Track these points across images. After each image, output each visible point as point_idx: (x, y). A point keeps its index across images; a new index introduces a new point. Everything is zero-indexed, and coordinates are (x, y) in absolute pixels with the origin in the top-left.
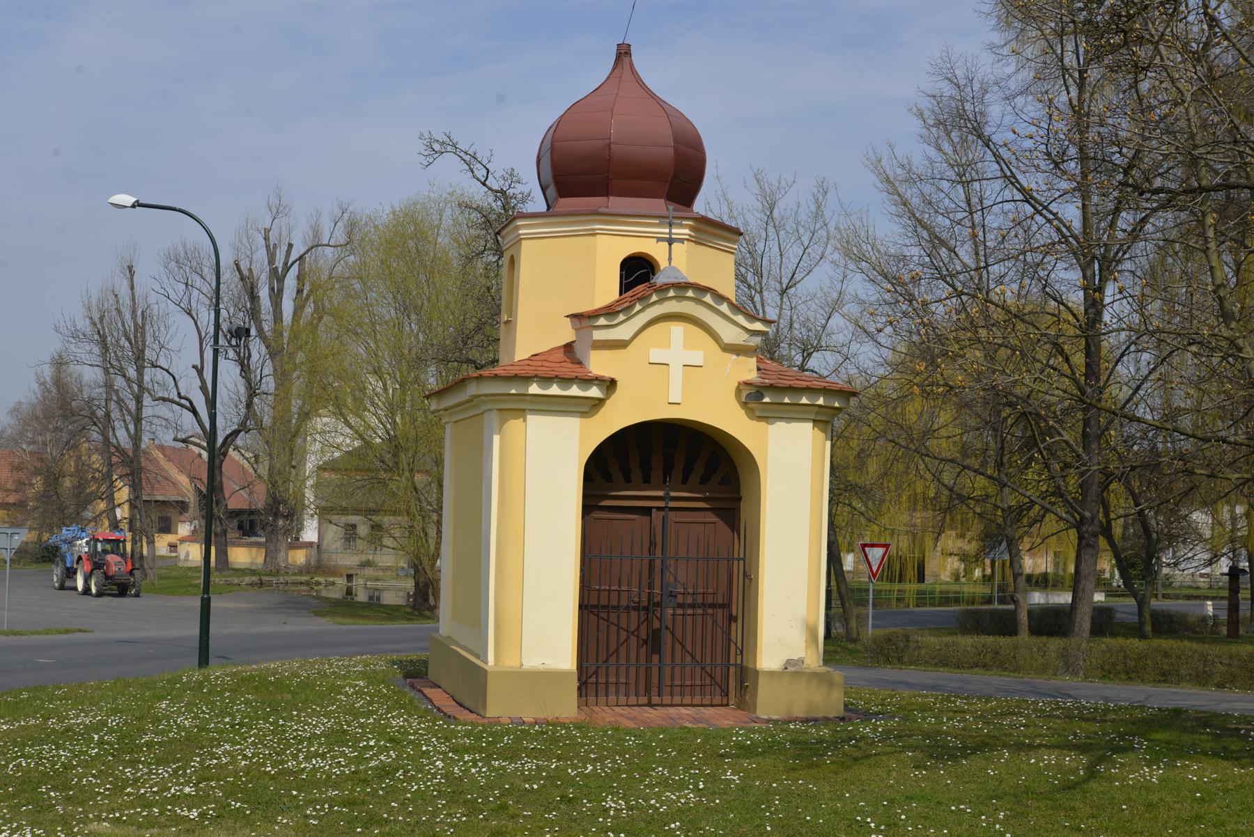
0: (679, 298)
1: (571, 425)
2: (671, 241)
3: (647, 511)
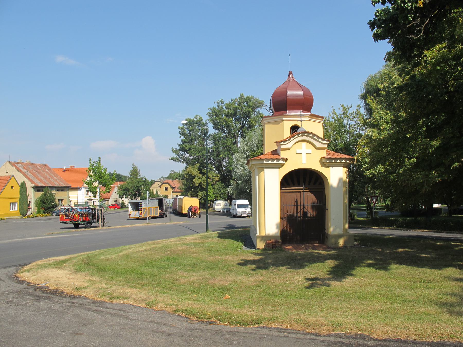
0: (307, 136)
1: (277, 170)
2: (301, 121)
3: (300, 192)
